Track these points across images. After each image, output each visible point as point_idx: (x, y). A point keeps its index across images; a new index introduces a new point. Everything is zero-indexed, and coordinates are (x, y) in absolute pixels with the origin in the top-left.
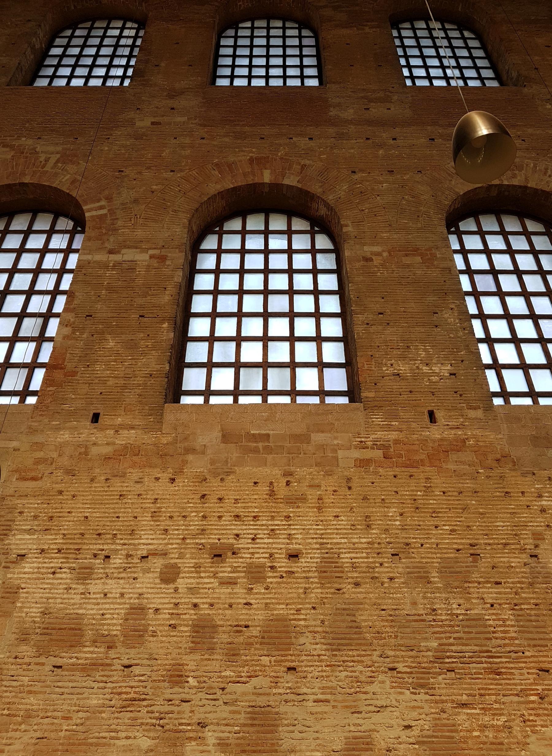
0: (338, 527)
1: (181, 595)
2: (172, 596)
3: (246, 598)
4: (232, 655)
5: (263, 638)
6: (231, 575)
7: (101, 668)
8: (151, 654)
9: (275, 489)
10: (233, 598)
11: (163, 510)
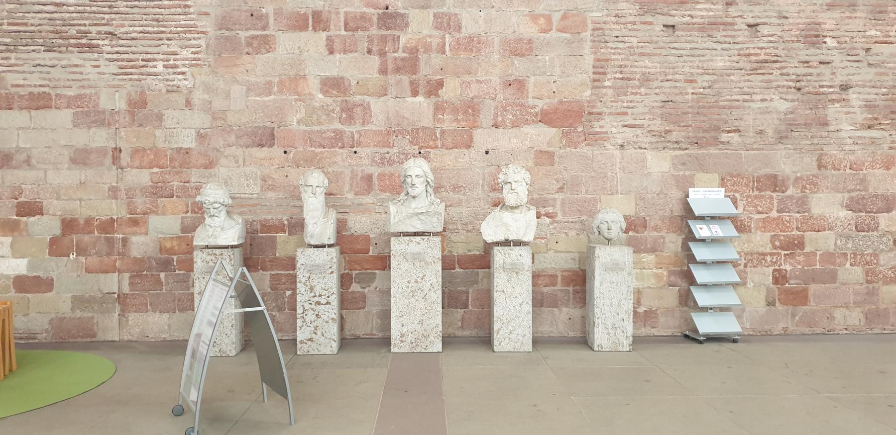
7: (722, 27)
8: (779, 12)
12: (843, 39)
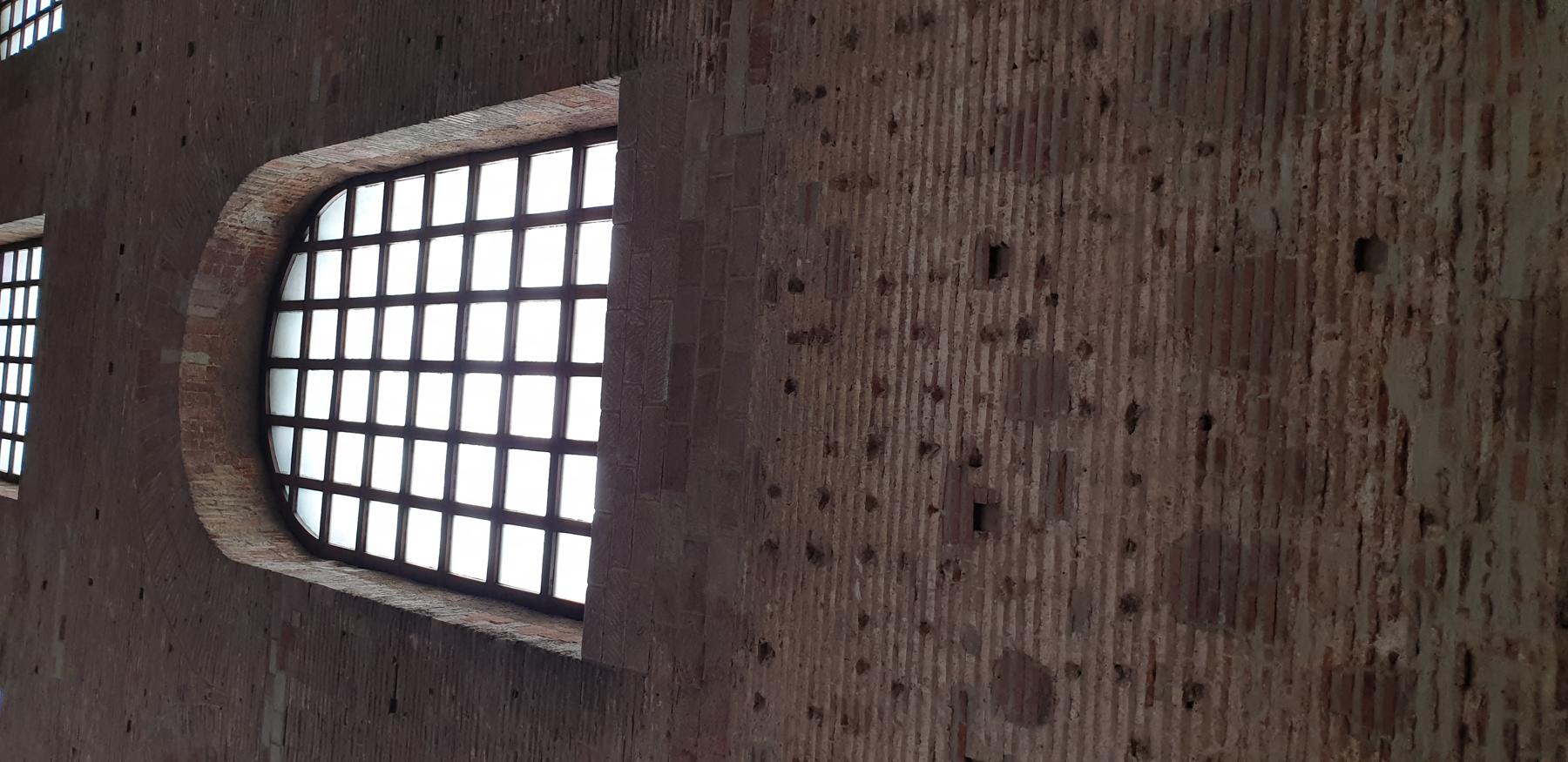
0: (920, 120)
1: (1092, 655)
2: (1091, 690)
3: (1112, 426)
4: (1302, 480)
5: (1246, 364)
6: (1036, 474)
9: (808, 328)
10: (1109, 472)
11: (840, 692)
12: (1384, 601)
